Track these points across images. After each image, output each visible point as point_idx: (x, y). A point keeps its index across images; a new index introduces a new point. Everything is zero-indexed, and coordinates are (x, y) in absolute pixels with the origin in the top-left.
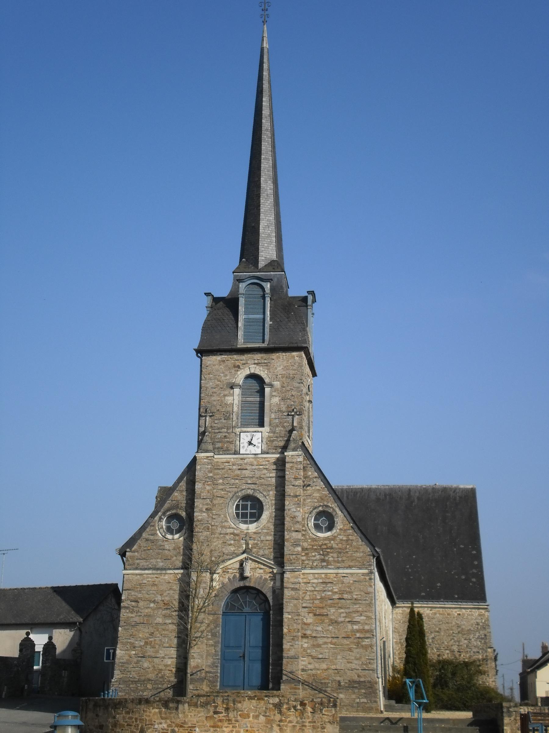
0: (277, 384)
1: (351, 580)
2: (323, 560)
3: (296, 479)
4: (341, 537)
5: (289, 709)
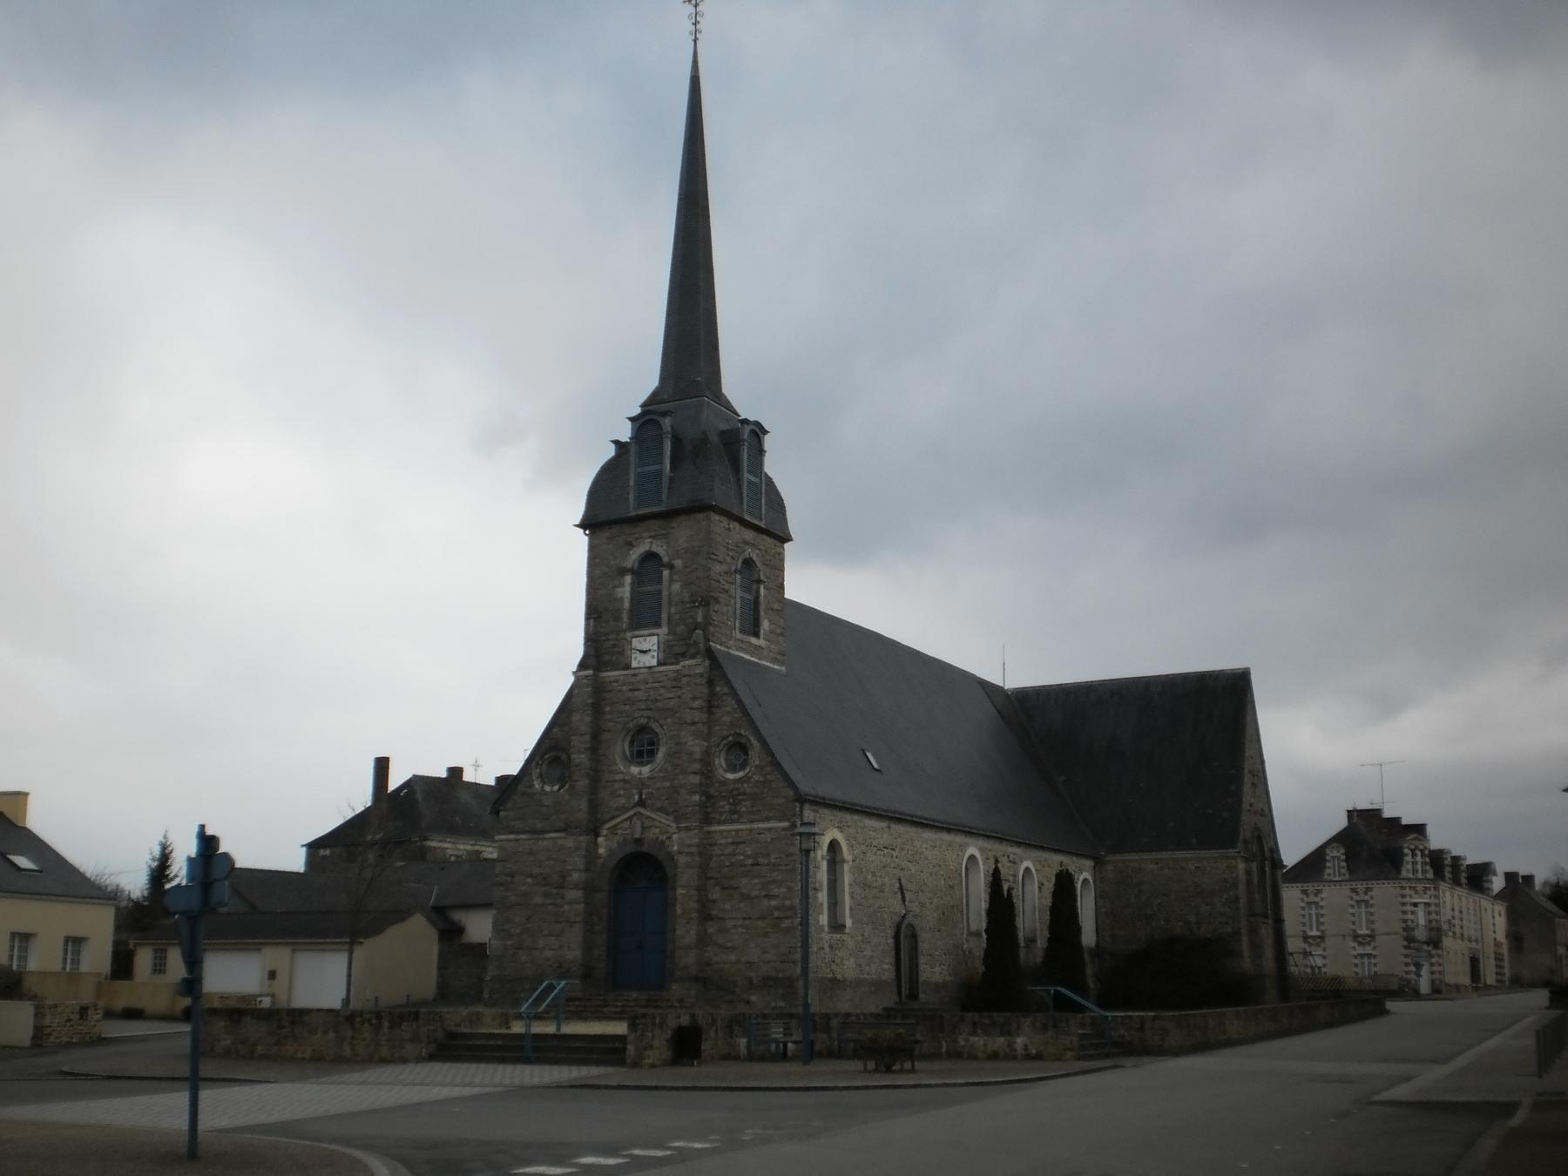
0: (678, 563)
1: (768, 837)
2: (733, 812)
3: (694, 698)
4: (756, 777)
5: (362, 1023)
